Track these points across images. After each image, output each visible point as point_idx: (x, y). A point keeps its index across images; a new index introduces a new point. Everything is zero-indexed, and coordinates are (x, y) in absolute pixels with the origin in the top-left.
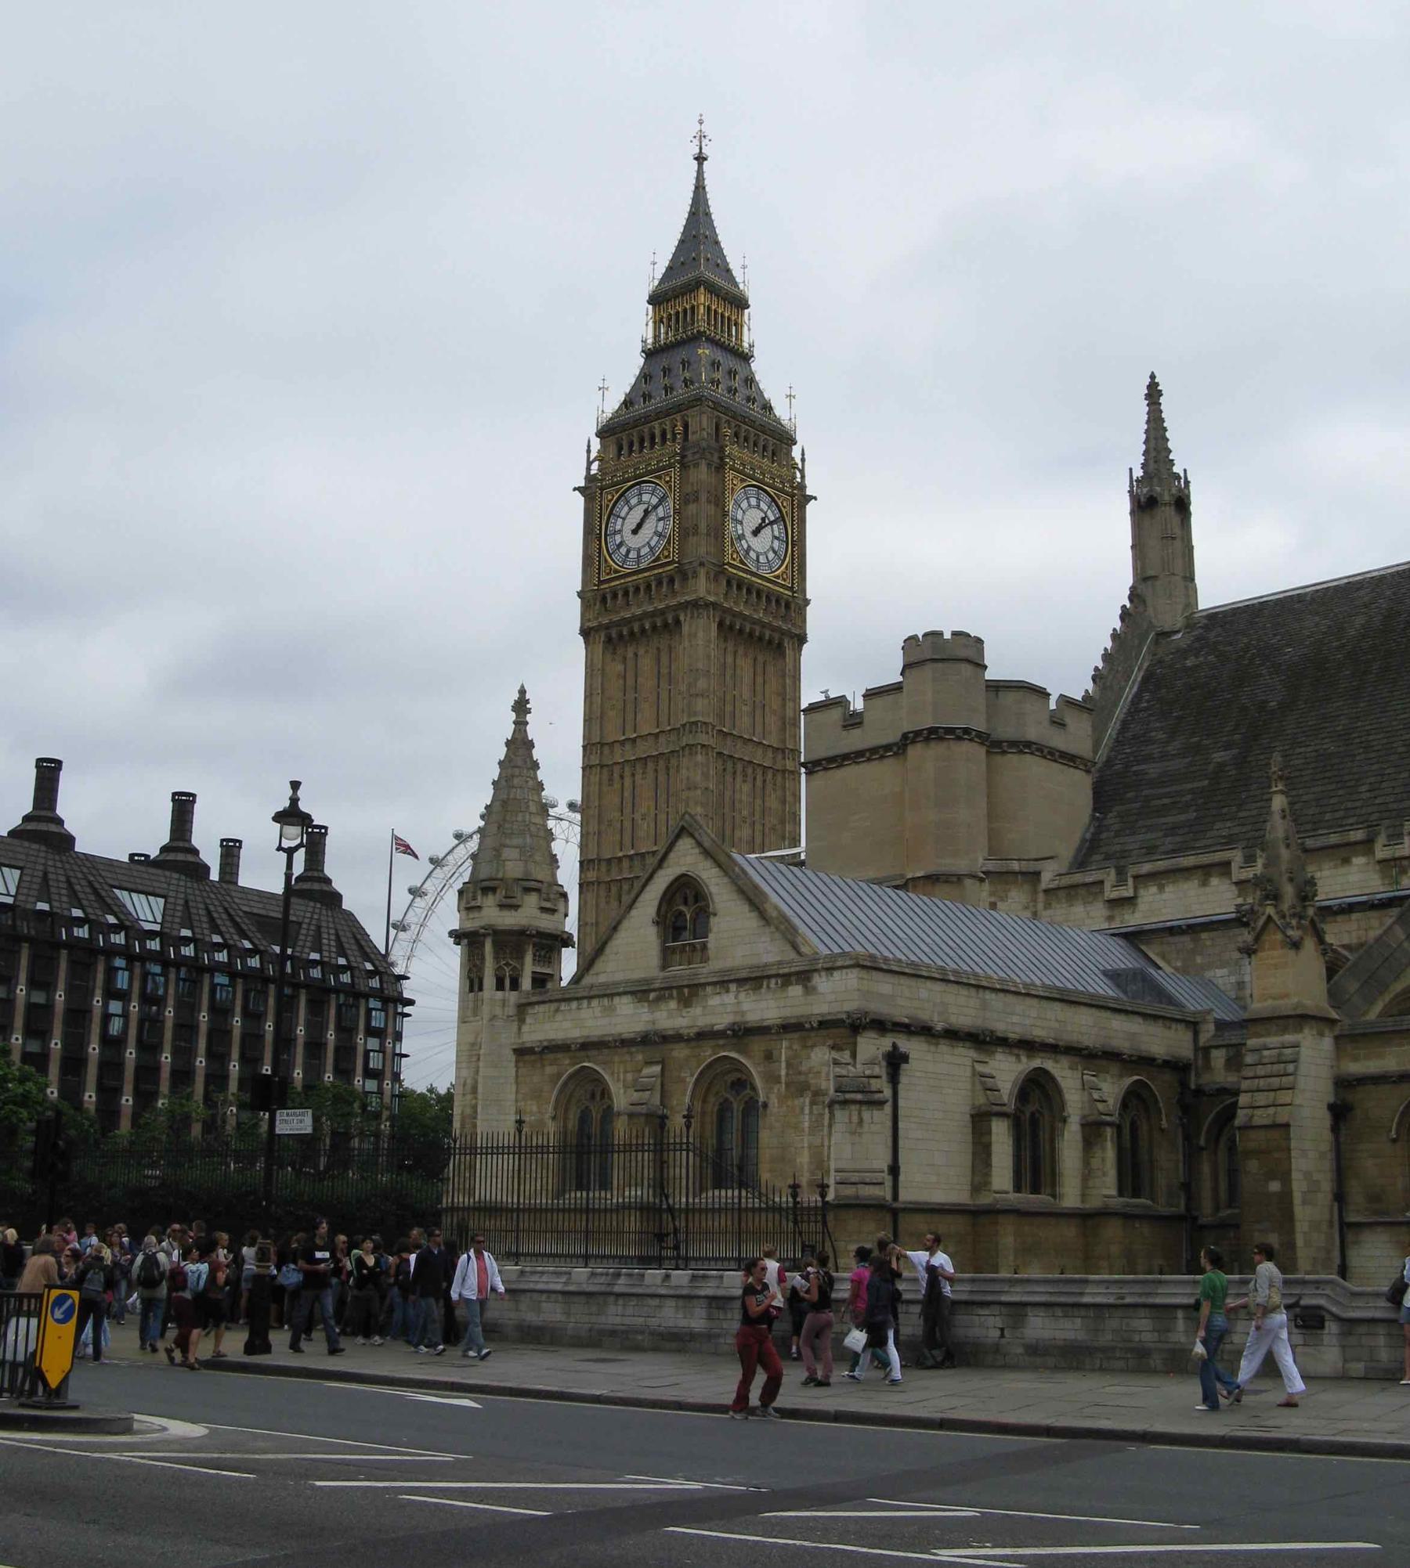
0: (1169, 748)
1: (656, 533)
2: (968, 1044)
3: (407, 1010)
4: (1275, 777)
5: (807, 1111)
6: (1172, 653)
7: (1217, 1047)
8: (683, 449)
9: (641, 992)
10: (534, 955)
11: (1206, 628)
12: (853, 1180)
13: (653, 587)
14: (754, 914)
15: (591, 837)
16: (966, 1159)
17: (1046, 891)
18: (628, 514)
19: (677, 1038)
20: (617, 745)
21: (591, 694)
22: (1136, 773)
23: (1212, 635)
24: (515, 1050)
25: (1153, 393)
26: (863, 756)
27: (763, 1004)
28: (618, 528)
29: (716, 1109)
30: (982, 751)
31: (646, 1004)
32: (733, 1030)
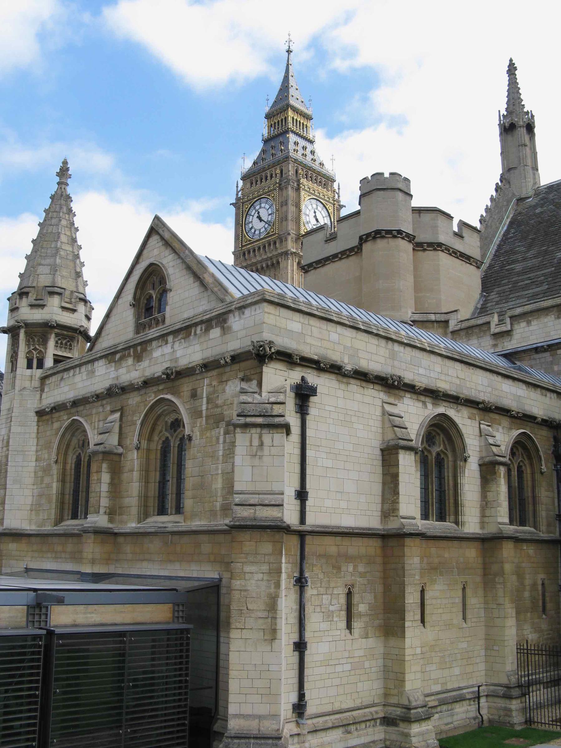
0: (527, 255)
2: (377, 387)
6: (527, 208)
10: (57, 342)
11: (546, 193)
12: (252, 502)
13: (267, 246)
14: (197, 284)
16: (377, 488)
17: (453, 332)
22: (507, 270)
23: (551, 196)
24: (37, 413)
27: (190, 350)
29: (159, 448)
30: (410, 247)
31: (113, 364)
32: (167, 375)
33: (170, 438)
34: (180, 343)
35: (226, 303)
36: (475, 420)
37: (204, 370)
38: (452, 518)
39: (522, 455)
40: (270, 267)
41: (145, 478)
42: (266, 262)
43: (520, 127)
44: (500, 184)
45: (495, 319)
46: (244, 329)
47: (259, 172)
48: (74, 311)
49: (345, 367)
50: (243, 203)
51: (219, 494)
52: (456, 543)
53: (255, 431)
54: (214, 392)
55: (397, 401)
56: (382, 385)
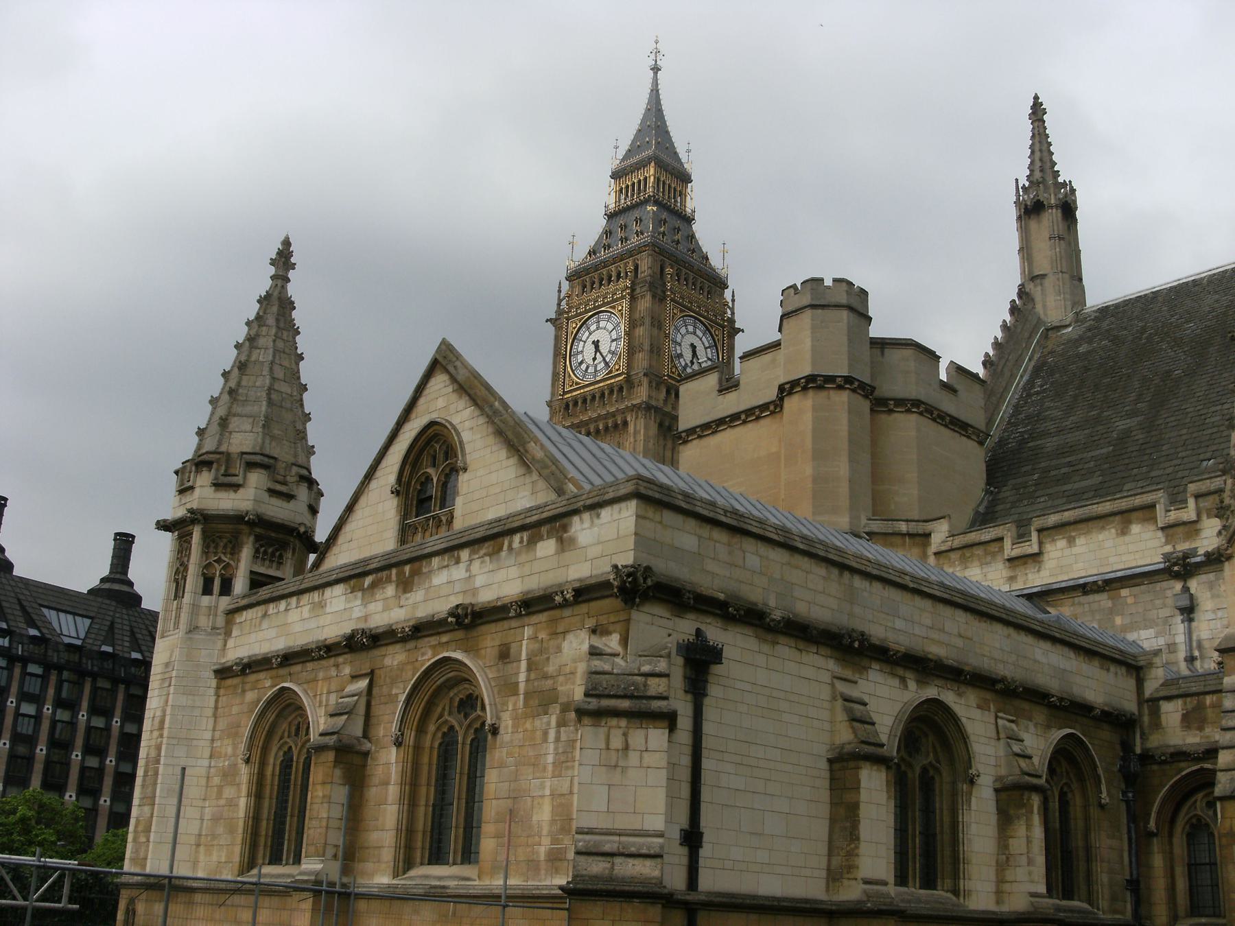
0: (1064, 424)
2: (823, 650)
5: (552, 735)
7: (1169, 698)
8: (633, 283)
10: (257, 551)
11: (1096, 319)
12: (607, 848)
16: (821, 829)
17: (937, 554)
18: (588, 338)
23: (1105, 325)
24: (217, 672)
25: (1037, 112)
26: (739, 418)
27: (501, 575)
29: (436, 745)
30: (865, 405)
31: (360, 594)
33: (457, 727)
34: (482, 562)
35: (567, 497)
36: (989, 711)
37: (523, 613)
39: (1068, 773)
40: (611, 429)
41: (410, 799)
42: (605, 421)
44: (1017, 302)
46: (598, 544)
47: (596, 268)
48: (289, 497)
49: (770, 614)
51: (545, 832)
54: (541, 651)
55: (857, 676)
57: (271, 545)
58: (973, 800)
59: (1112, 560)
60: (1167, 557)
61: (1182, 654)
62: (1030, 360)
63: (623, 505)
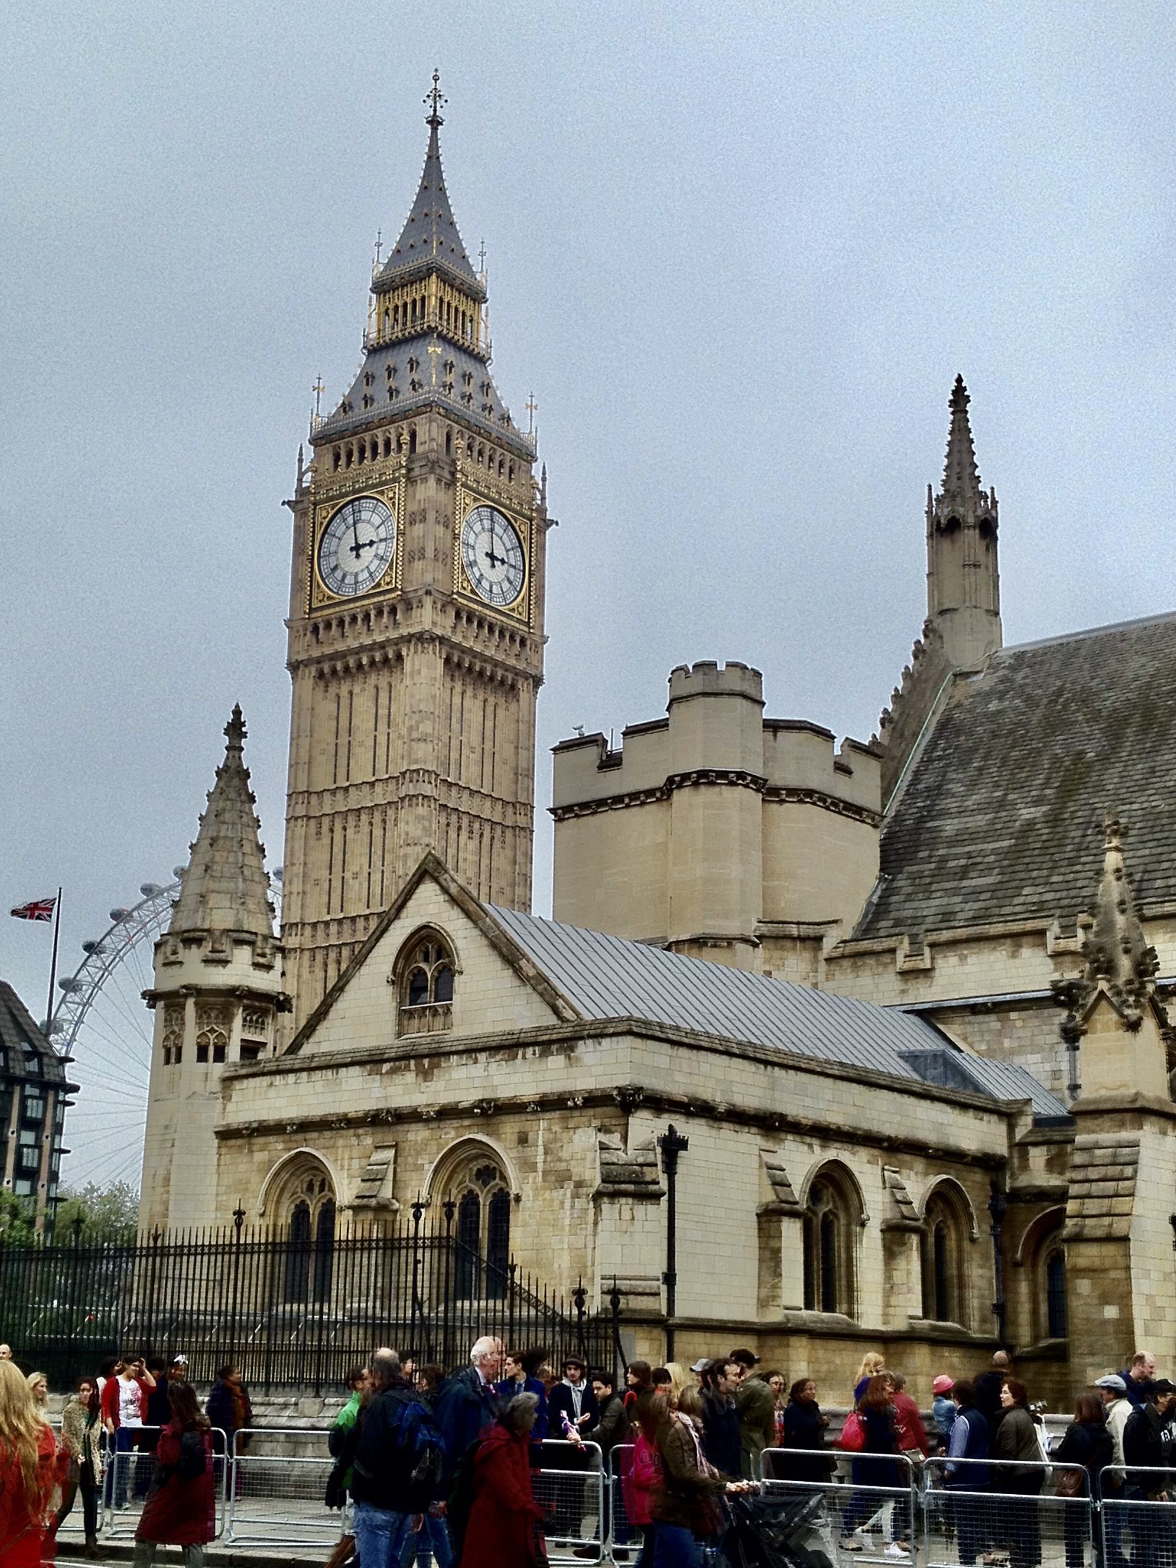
0: (967, 803)
1: (376, 556)
2: (754, 1130)
3: (70, 1097)
4: (1108, 831)
5: (568, 1204)
6: (971, 697)
7: (1036, 1144)
8: (410, 460)
9: (372, 1061)
10: (245, 1020)
11: (1013, 668)
15: (294, 897)
17: (829, 960)
19: (412, 1116)
20: (327, 795)
21: (299, 736)
24: (217, 1133)
25: (959, 399)
26: (622, 802)
27: (515, 1078)
28: (332, 549)
31: (378, 1077)
32: (482, 1109)
38: (844, 1307)
40: (379, 665)
43: (969, 527)
44: (923, 641)
45: (905, 947)
48: (269, 967)
50: (315, 504)
51: (565, 1275)
52: (850, 1345)
53: (625, 1203)
56: (758, 1127)
57: (255, 1013)
58: (865, 1239)
59: (1002, 982)
60: (1055, 986)
61: (1066, 1082)
62: (934, 713)
63: (620, 1038)
